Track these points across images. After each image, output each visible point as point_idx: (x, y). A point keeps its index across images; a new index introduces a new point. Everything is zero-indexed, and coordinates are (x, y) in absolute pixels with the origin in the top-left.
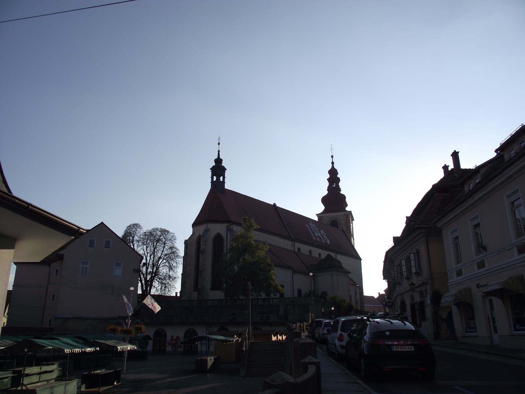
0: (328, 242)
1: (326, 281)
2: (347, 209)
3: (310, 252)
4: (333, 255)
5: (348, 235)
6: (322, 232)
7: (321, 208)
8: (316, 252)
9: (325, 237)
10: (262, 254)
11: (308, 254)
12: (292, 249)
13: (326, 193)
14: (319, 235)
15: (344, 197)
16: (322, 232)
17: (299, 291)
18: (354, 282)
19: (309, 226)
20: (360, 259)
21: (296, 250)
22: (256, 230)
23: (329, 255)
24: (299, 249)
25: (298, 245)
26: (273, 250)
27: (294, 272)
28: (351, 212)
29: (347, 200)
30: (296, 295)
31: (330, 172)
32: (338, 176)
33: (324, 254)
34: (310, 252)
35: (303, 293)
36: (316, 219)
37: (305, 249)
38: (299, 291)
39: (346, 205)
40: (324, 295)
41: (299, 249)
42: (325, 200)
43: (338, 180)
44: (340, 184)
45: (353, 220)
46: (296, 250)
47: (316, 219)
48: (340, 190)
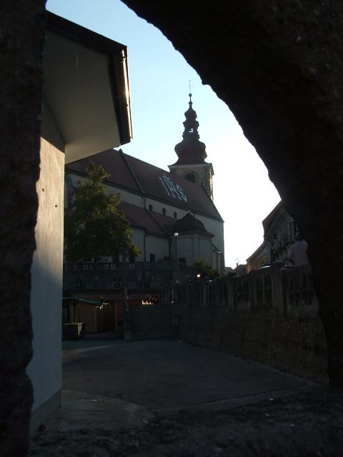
0: (186, 200)
1: (185, 245)
2: (206, 160)
3: (164, 210)
4: (192, 214)
5: (207, 191)
6: (178, 187)
7: (174, 158)
8: (170, 211)
9: (181, 193)
10: (112, 209)
11: (162, 213)
12: (142, 206)
13: (180, 139)
14: (175, 190)
15: (202, 146)
16: (178, 187)
17: (152, 257)
18: (216, 248)
19: (163, 178)
20: (221, 221)
21: (148, 208)
22: (106, 182)
23: (188, 214)
24: (151, 207)
25: (149, 202)
26: (124, 206)
27: (147, 234)
28: (211, 164)
29: (207, 150)
30: (148, 259)
31: (186, 114)
32: (197, 120)
33: (181, 214)
34: (164, 210)
35: (157, 259)
36: (168, 170)
37: (158, 207)
38: (152, 257)
39: (206, 156)
40: (183, 260)
41: (151, 207)
42: (179, 149)
43: (197, 124)
44: (199, 129)
45: (213, 174)
46: (148, 208)
47: (168, 170)
48: (198, 137)
